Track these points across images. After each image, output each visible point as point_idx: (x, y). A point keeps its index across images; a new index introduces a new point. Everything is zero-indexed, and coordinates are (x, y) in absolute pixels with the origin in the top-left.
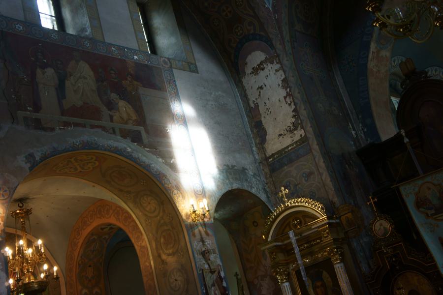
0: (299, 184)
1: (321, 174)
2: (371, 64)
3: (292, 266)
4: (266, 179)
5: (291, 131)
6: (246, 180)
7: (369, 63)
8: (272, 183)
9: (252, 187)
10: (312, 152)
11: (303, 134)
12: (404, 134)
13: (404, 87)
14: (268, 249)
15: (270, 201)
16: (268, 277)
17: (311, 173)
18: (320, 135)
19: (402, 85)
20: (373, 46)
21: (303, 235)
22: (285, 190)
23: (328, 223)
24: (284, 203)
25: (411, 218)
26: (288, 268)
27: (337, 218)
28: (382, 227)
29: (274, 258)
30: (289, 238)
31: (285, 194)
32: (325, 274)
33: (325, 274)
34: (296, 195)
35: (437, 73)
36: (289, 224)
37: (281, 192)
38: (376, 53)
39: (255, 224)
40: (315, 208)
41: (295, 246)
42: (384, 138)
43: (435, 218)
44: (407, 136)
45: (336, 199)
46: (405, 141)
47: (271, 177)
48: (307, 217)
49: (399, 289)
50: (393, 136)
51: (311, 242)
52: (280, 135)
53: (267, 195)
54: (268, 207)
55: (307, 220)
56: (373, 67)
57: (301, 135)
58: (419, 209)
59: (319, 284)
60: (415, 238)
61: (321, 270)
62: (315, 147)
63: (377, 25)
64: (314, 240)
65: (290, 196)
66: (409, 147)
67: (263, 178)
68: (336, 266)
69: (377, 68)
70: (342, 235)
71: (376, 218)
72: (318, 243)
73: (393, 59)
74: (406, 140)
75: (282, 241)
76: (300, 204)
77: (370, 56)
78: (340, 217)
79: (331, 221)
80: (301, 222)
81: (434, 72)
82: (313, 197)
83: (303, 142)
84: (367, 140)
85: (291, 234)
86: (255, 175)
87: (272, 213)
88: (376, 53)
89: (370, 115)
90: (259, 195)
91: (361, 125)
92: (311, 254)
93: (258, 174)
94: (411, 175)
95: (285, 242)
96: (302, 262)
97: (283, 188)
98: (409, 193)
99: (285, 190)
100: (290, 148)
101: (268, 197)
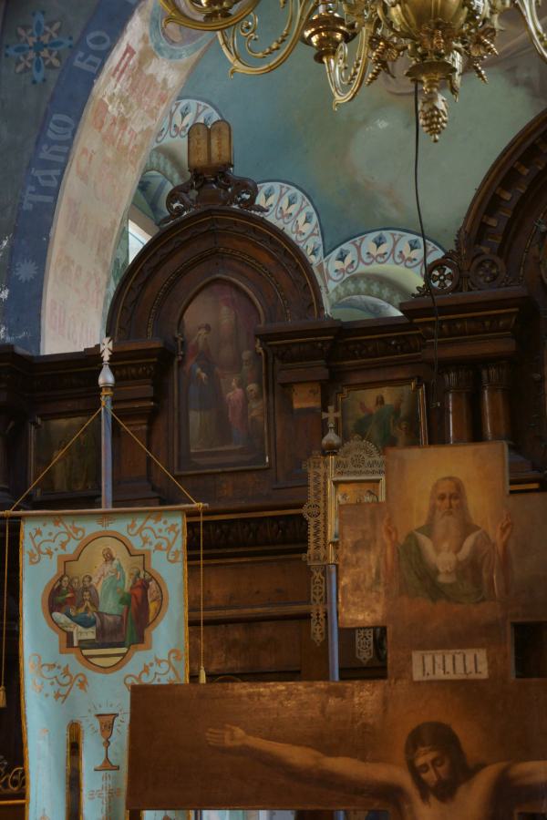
2: (108, 87)
7: (103, 77)
12: (106, 356)
13: (175, 206)
19: (173, 197)
20: (136, 31)
35: (293, 209)
38: (136, 57)
42: (53, 345)
43: (87, 657)
44: (113, 369)
46: (101, 381)
56: (111, 99)
58: (51, 611)
63: (314, 39)
69: (123, 110)
73: (184, 103)
74: (106, 377)
77: (116, 56)
81: (285, 202)
88: (136, 57)
89: (40, 257)
94: (79, 498)
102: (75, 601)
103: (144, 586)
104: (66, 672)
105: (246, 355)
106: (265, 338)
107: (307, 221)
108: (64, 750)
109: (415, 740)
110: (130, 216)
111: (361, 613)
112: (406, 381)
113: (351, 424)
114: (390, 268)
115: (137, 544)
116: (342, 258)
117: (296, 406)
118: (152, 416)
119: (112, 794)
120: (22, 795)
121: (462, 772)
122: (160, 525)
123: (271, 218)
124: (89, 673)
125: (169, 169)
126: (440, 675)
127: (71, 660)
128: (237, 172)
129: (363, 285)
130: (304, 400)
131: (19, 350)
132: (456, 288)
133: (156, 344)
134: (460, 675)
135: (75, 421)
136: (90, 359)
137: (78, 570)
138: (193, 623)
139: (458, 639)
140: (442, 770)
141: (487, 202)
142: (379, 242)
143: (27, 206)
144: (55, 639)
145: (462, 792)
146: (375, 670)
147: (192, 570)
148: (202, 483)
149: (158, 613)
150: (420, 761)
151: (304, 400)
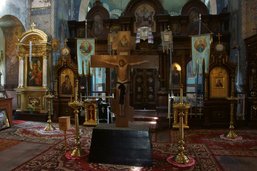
0: (41, 24)
1: (51, 24)
3: (27, 55)
4: (28, 17)
5: (45, 2)
6: (19, 14)
8: (30, 19)
9: (20, 18)
10: (51, 14)
11: (50, 5)
12: (86, 21)
14: (19, 45)
15: (26, 27)
16: (15, 56)
17: (47, 22)
18: (57, 9)
19: (93, 4)
21: (35, 44)
22: (34, 24)
23: (47, 43)
24: (32, 29)
25: (76, 52)
26: (25, 55)
27: (51, 43)
28: (66, 52)
29: (20, 50)
30: (29, 44)
31: (34, 26)
32: (39, 62)
33: (39, 62)
34: (38, 28)
36: (31, 39)
37: (32, 24)
39: (17, 34)
40: (44, 36)
41: (31, 47)
44: (87, 23)
45: (53, 36)
47: (30, 17)
48: (39, 38)
49: (63, 74)
50: (83, 21)
51: (37, 48)
52: (40, 1)
53: (26, 24)
54: (24, 28)
55: (39, 39)
57: (49, 5)
59: (35, 64)
60: (75, 58)
61: (38, 60)
62: (53, 12)
64: (39, 48)
65: (36, 28)
66: (86, 26)
67: (26, 16)
68: (44, 60)
70: (50, 50)
71: (65, 47)
72: (40, 49)
74: (86, 24)
75: (26, 44)
76: (38, 32)
78: (52, 43)
79: (48, 43)
80: (36, 39)
81: (105, 5)
82: (44, 32)
83: (49, 9)
84: (73, 19)
85: (31, 42)
86: (23, 13)
87: (25, 31)
89: (78, 10)
90: (22, 22)
91: (73, 12)
92: (36, 53)
93: (25, 13)
94: (83, 37)
95: (27, 45)
96: (31, 54)
97: (33, 23)
98: (79, 42)
99: (34, 24)
100: (42, 9)
101: (26, 25)
102: (83, 48)
103: (90, 47)
104: (82, 55)
105: (101, 22)
106: (103, 20)
107: (108, 7)
108: (82, 64)
109: (120, 61)
110: (88, 6)
111: (114, 48)
112: (119, 26)
113: (113, 30)
114: (117, 13)
115: (89, 42)
116: (112, 12)
117: (107, 28)
118: (91, 29)
119: (87, 68)
120: (78, 68)
121: (124, 64)
122: (92, 40)
123: (104, 7)
124: (84, 55)
125: (93, 1)
126: (123, 55)
127: (82, 54)
128: (101, 1)
129: (114, 15)
130: (107, 27)
131: (76, 21)
132: (125, 16)
133: (91, 21)
134: (125, 55)
135: (82, 29)
136: (84, 22)
137: (83, 45)
138: (95, 51)
139: (125, 51)
140: (122, 64)
141: (128, 6)
142: (116, 10)
143: (77, 5)
144: (81, 52)
145: (124, 66)
146: (116, 54)
147: (95, 45)
148: (96, 36)
149: (92, 49)
150: (120, 63)
151: (107, 27)
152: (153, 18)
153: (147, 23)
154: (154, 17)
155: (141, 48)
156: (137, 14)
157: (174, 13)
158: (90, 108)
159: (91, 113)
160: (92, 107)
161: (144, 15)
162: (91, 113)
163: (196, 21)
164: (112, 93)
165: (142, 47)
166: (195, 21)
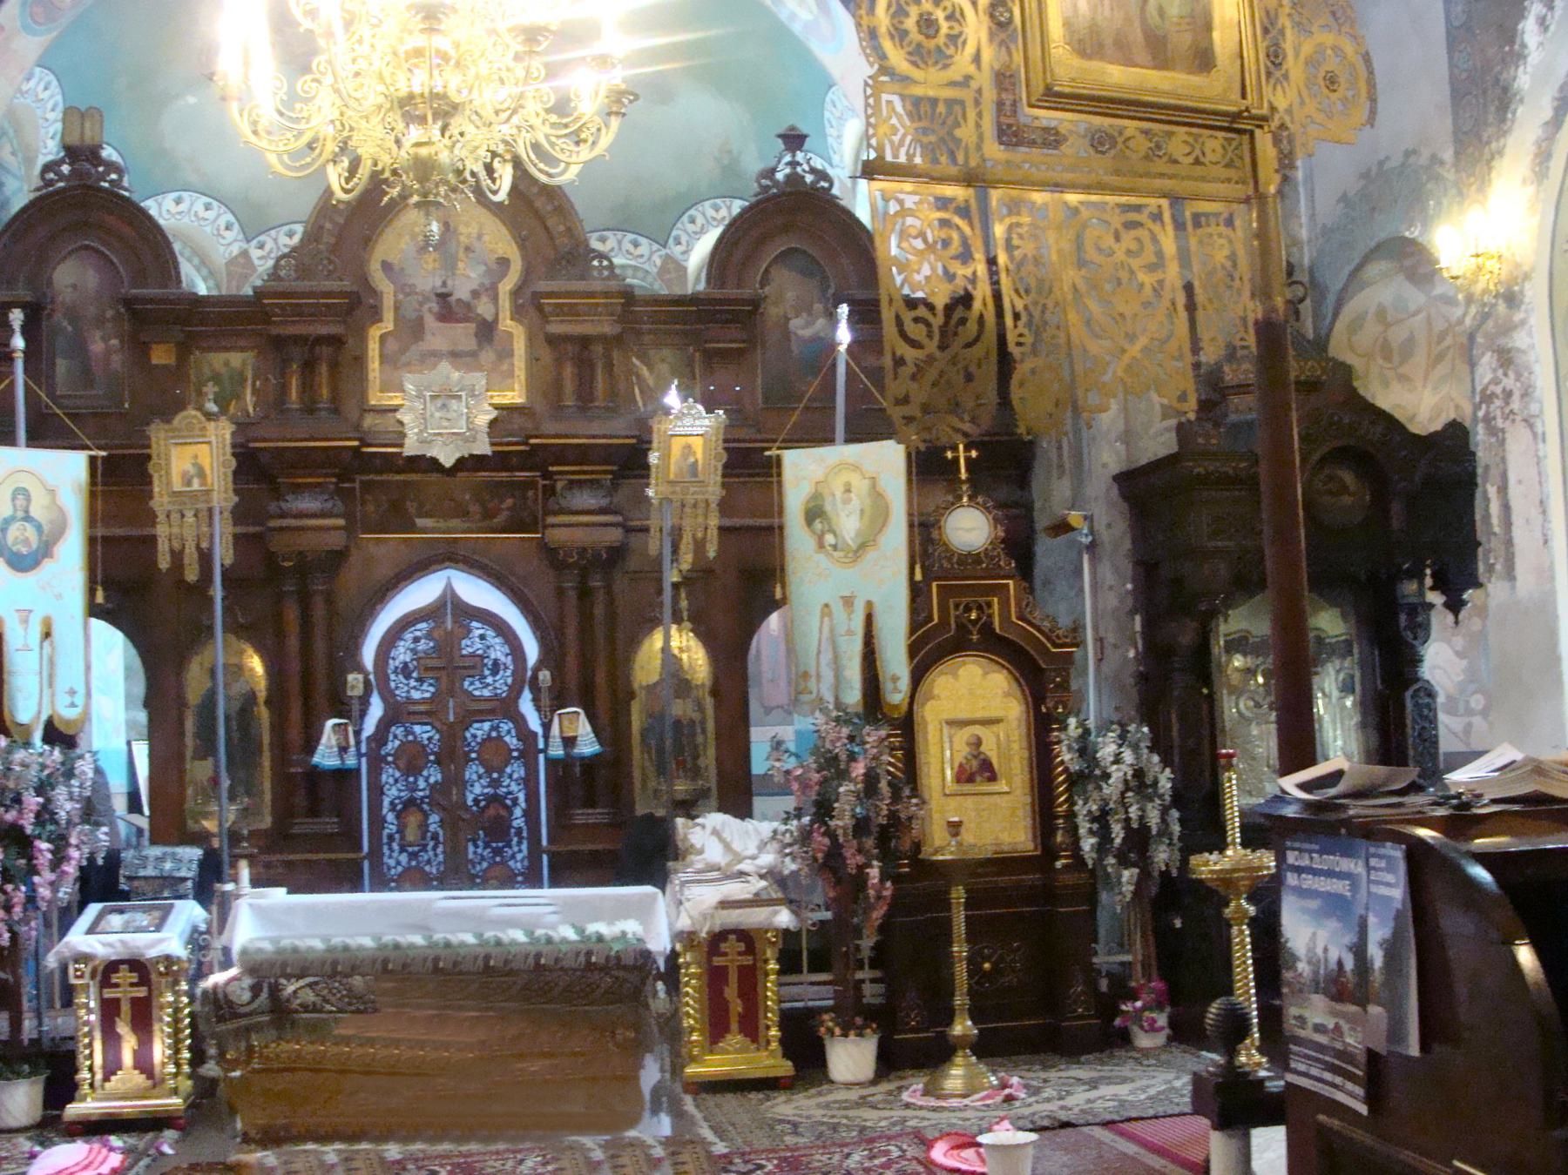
105: (109, 314)
117: (155, 361)
130: (161, 356)
142: (178, 201)
152: (505, 303)
153: (463, 334)
154: (516, 293)
155: (420, 522)
156: (387, 267)
157: (627, 246)
158: (117, 985)
159: (731, 992)
160: (134, 977)
161: (450, 283)
162: (731, 992)
163: (807, 333)
164: (233, 865)
165: (428, 515)
166: (800, 332)
